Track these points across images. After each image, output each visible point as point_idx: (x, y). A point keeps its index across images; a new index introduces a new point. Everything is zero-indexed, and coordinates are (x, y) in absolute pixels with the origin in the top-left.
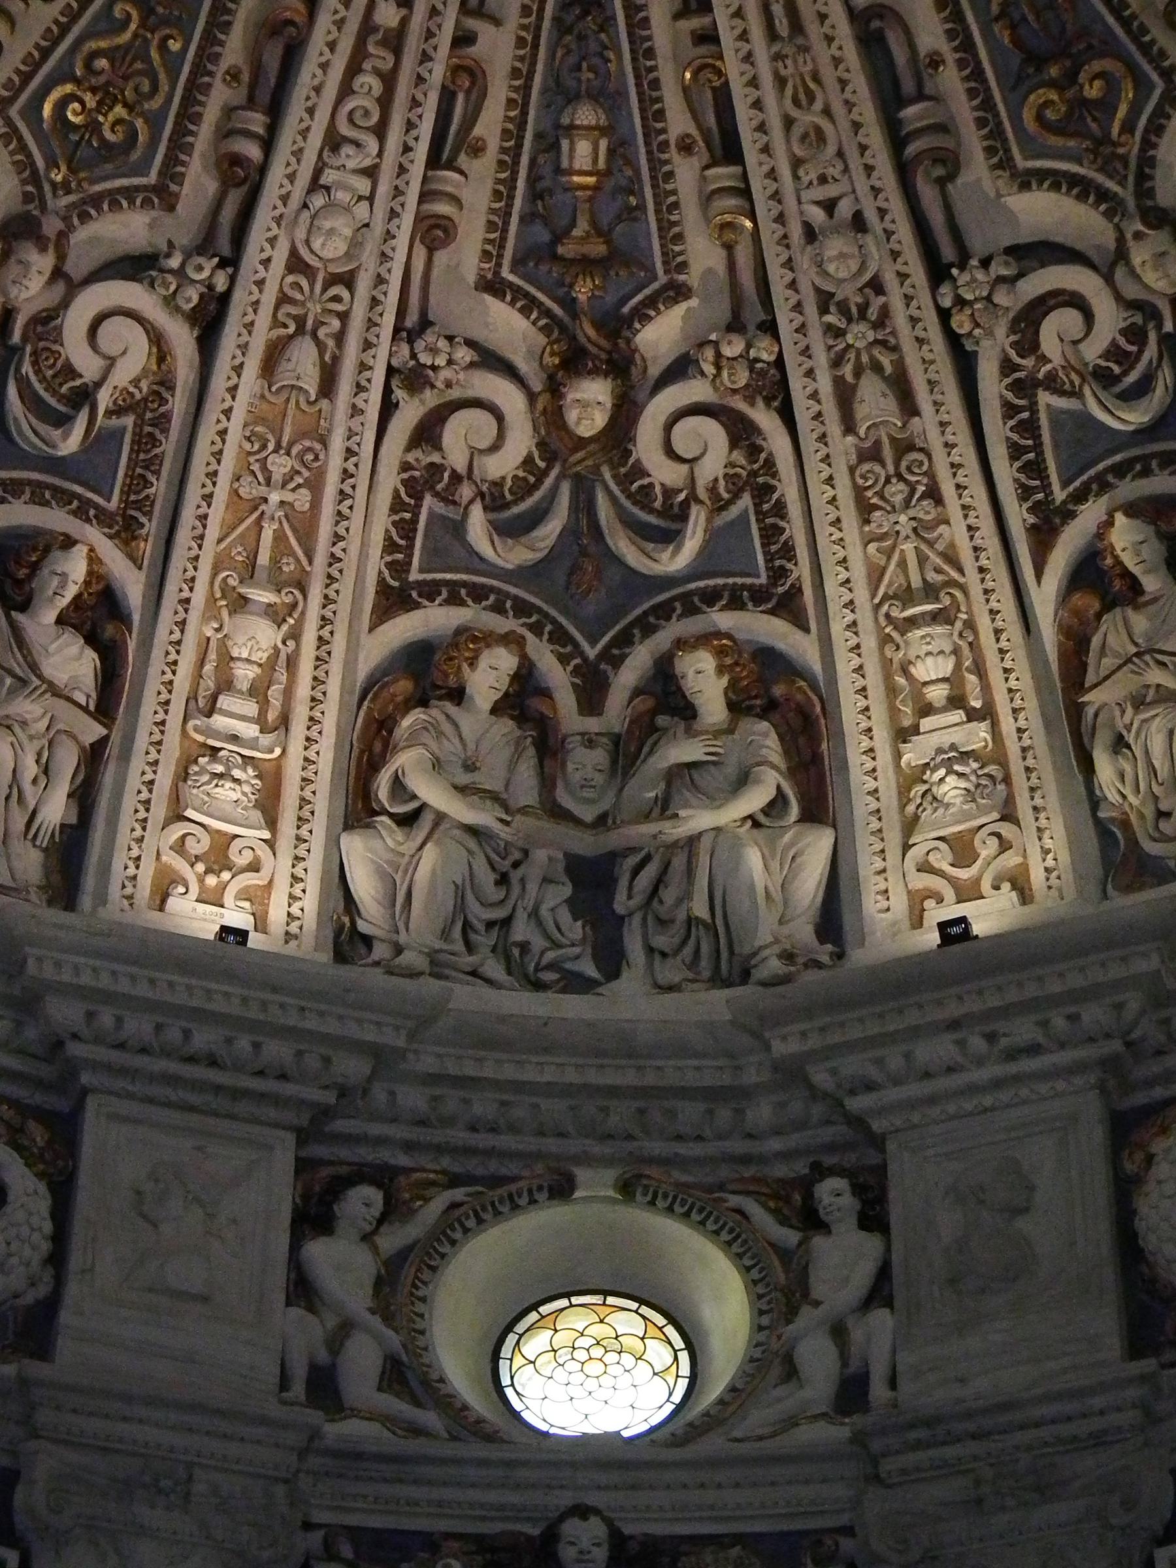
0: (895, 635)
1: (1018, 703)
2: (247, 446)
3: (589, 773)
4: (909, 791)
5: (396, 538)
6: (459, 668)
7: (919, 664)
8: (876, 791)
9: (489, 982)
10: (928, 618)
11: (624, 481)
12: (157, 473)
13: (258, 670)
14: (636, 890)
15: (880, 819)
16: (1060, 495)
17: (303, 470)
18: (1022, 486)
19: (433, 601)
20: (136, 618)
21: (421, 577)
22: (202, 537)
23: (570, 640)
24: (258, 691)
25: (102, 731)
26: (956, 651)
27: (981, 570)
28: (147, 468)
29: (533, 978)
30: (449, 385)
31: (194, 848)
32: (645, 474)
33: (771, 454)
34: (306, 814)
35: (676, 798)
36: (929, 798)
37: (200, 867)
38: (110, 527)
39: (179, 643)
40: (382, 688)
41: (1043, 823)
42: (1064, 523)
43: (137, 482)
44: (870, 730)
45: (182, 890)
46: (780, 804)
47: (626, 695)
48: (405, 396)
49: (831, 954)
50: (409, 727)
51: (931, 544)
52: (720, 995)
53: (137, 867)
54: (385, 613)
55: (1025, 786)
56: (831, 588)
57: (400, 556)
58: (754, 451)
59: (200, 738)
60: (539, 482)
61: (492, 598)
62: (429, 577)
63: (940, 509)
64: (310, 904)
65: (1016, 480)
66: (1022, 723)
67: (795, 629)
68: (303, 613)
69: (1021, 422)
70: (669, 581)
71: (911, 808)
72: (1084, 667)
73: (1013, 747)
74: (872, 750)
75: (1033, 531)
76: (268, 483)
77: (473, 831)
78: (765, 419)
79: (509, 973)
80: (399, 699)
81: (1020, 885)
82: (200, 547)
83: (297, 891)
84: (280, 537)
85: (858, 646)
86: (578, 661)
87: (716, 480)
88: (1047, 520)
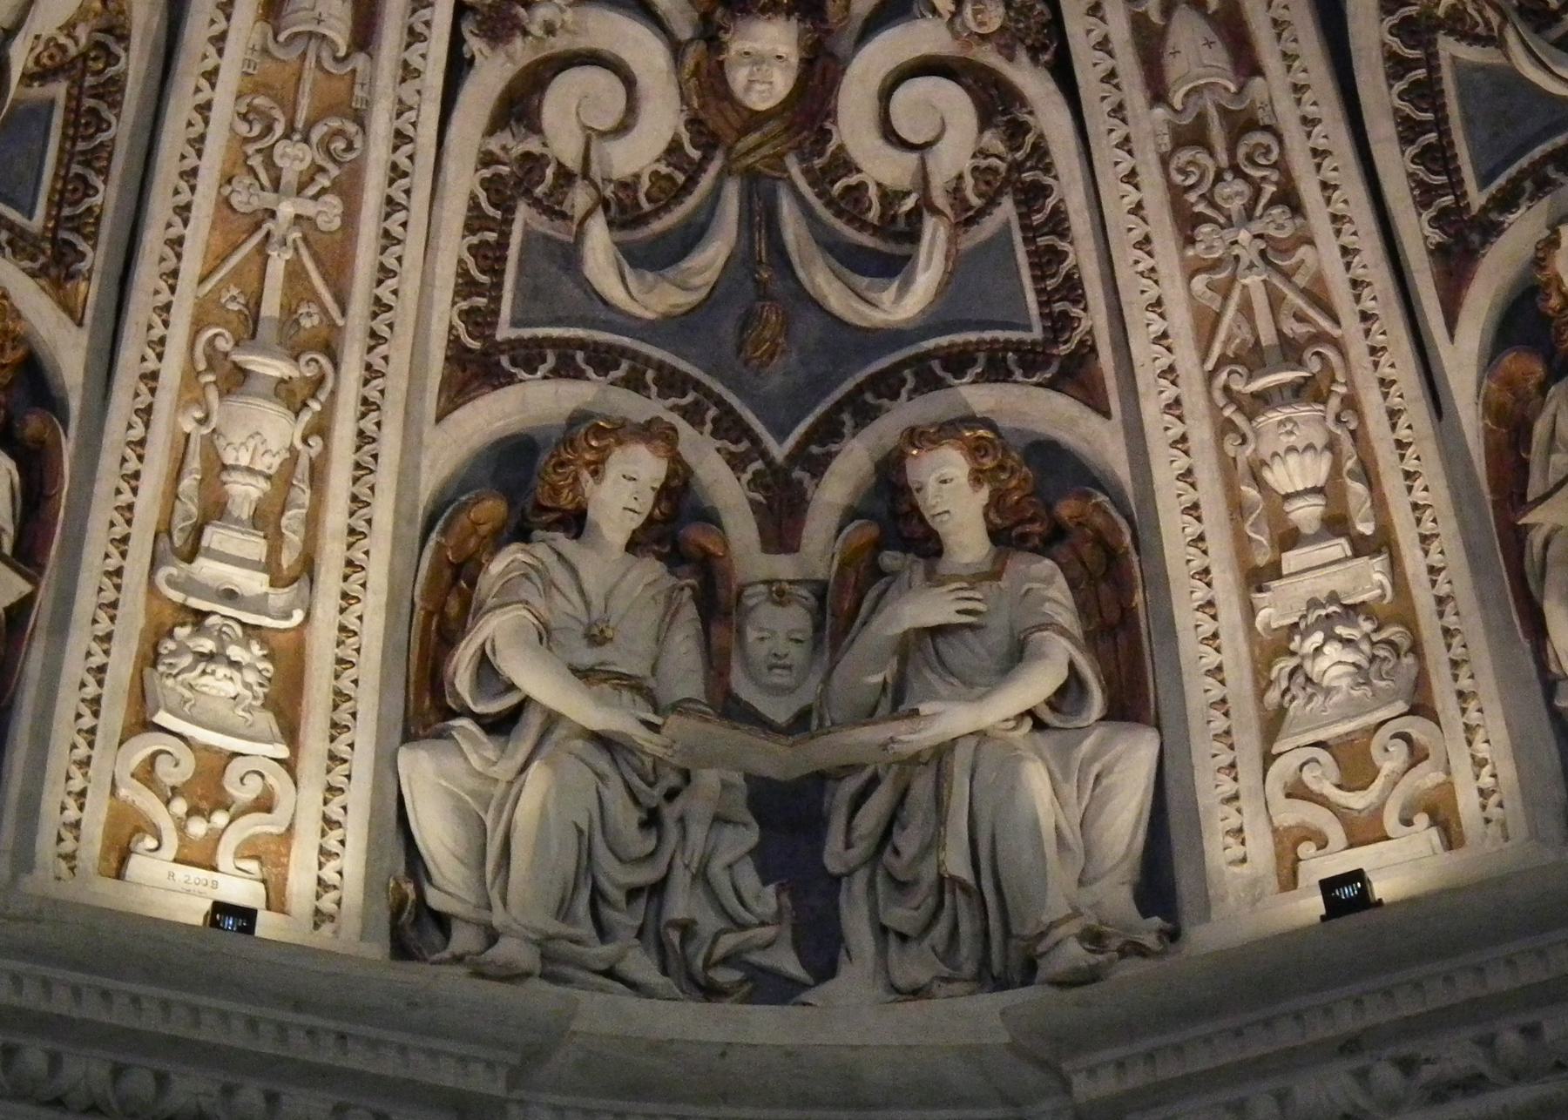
0: (1240, 420)
1: (1428, 527)
2: (243, 128)
3: (782, 646)
4: (1269, 667)
5: (475, 272)
6: (576, 479)
7: (1277, 466)
8: (1219, 668)
9: (634, 986)
10: (1287, 393)
11: (821, 180)
12: (104, 172)
13: (264, 485)
14: (856, 834)
15: (1226, 714)
16: (1477, 198)
17: (330, 166)
18: (1420, 183)
19: (533, 371)
20: (75, 404)
21: (513, 334)
22: (175, 274)
23: (747, 432)
24: (265, 520)
25: (22, 587)
26: (1332, 445)
27: (1365, 317)
28: (87, 164)
29: (702, 982)
30: (550, 29)
31: (169, 774)
32: (850, 167)
33: (1041, 136)
34: (343, 717)
35: (915, 686)
36: (1300, 679)
37: (180, 806)
38: (33, 259)
39: (142, 443)
40: (457, 512)
41: (1473, 717)
42: (1485, 242)
43: (73, 188)
44: (1206, 571)
45: (151, 843)
46: (1072, 695)
47: (833, 519)
48: (486, 50)
49: (1161, 932)
50: (502, 574)
51: (1287, 276)
52: (990, 1004)
53: (81, 808)
54: (460, 392)
55: (1445, 657)
56: (1140, 347)
57: (481, 301)
58: (1016, 131)
59: (177, 596)
60: (692, 181)
61: (625, 365)
62: (527, 333)
63: (1299, 221)
64: (352, 863)
65: (1411, 175)
66: (1435, 559)
67: (1088, 412)
68: (333, 393)
69: (1416, 84)
70: (894, 337)
71: (1273, 696)
72: (1524, 467)
73: (1423, 599)
74: (1210, 603)
75: (1438, 253)
76: (276, 188)
77: (602, 740)
78: (1031, 81)
79: (665, 971)
80: (484, 529)
81: (1442, 815)
82: (173, 289)
83: (332, 843)
84: (295, 273)
85: (1184, 438)
86: (758, 465)
87: (960, 177)
88: (1460, 237)
